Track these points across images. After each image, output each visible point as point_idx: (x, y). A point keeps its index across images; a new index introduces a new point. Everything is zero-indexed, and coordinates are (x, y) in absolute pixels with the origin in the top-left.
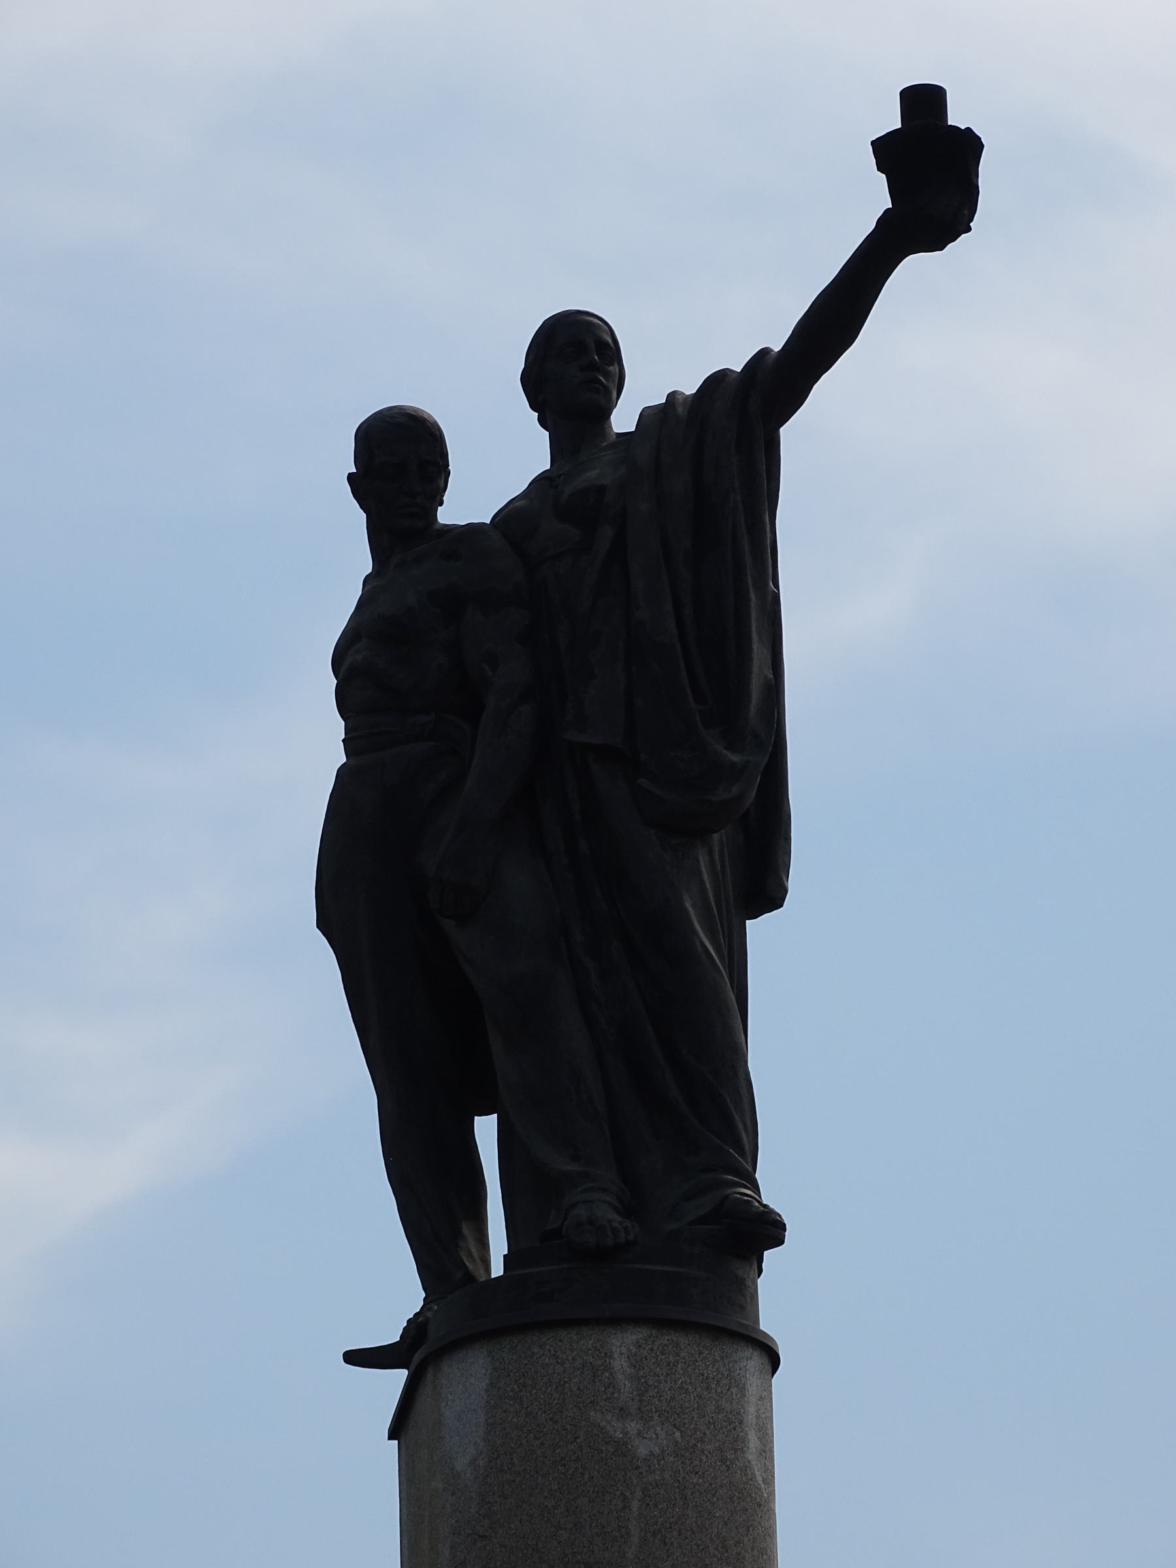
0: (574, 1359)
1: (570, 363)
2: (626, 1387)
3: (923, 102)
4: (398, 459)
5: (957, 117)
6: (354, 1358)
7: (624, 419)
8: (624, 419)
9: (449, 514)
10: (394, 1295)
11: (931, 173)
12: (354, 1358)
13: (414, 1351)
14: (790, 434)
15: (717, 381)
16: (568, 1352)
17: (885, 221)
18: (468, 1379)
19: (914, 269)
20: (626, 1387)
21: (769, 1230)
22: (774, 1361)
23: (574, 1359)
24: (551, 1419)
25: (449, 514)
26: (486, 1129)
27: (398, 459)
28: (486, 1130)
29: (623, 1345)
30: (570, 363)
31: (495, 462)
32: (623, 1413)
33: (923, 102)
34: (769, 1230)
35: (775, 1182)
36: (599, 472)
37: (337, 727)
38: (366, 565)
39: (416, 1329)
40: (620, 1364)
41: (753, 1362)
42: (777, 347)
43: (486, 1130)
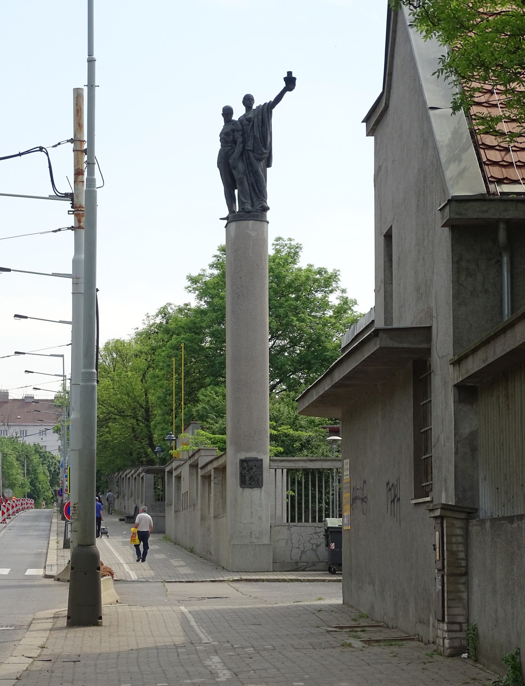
1: (248, 100)
2: (251, 228)
3: (290, 73)
4: (227, 112)
5: (293, 76)
6: (220, 219)
7: (254, 107)
10: (226, 212)
11: (290, 82)
12: (220, 219)
14: (274, 110)
15: (265, 104)
17: (285, 88)
18: (233, 225)
19: (288, 93)
20: (251, 228)
21: (268, 209)
22: (268, 223)
27: (227, 112)
28: (236, 191)
29: (251, 223)
30: (248, 100)
31: (239, 112)
32: (251, 231)
33: (290, 73)
34: (268, 209)
35: (270, 202)
36: (251, 115)
37: (220, 144)
40: (250, 225)
41: (266, 223)
42: (272, 100)
43: (236, 191)
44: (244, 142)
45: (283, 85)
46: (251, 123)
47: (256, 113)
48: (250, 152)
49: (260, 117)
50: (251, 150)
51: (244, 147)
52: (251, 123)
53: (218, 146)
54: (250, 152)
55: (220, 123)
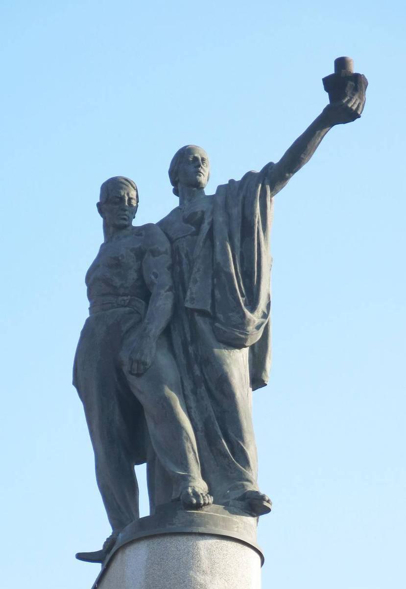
0: (184, 549)
3: (341, 63)
4: (115, 200)
8: (210, 190)
9: (138, 222)
10: (98, 530)
13: (106, 556)
16: (182, 546)
17: (327, 110)
19: (337, 132)
23: (184, 549)
24: (174, 573)
25: (138, 222)
26: (141, 471)
27: (115, 200)
28: (141, 471)
33: (341, 63)
38: (101, 239)
39: (110, 544)
44: (179, 286)
45: (323, 100)
46: (205, 227)
47: (220, 200)
48: (199, 320)
49: (236, 211)
50: (203, 313)
51: (177, 306)
52: (205, 227)
53: (78, 310)
54: (199, 320)
55: (90, 237)
